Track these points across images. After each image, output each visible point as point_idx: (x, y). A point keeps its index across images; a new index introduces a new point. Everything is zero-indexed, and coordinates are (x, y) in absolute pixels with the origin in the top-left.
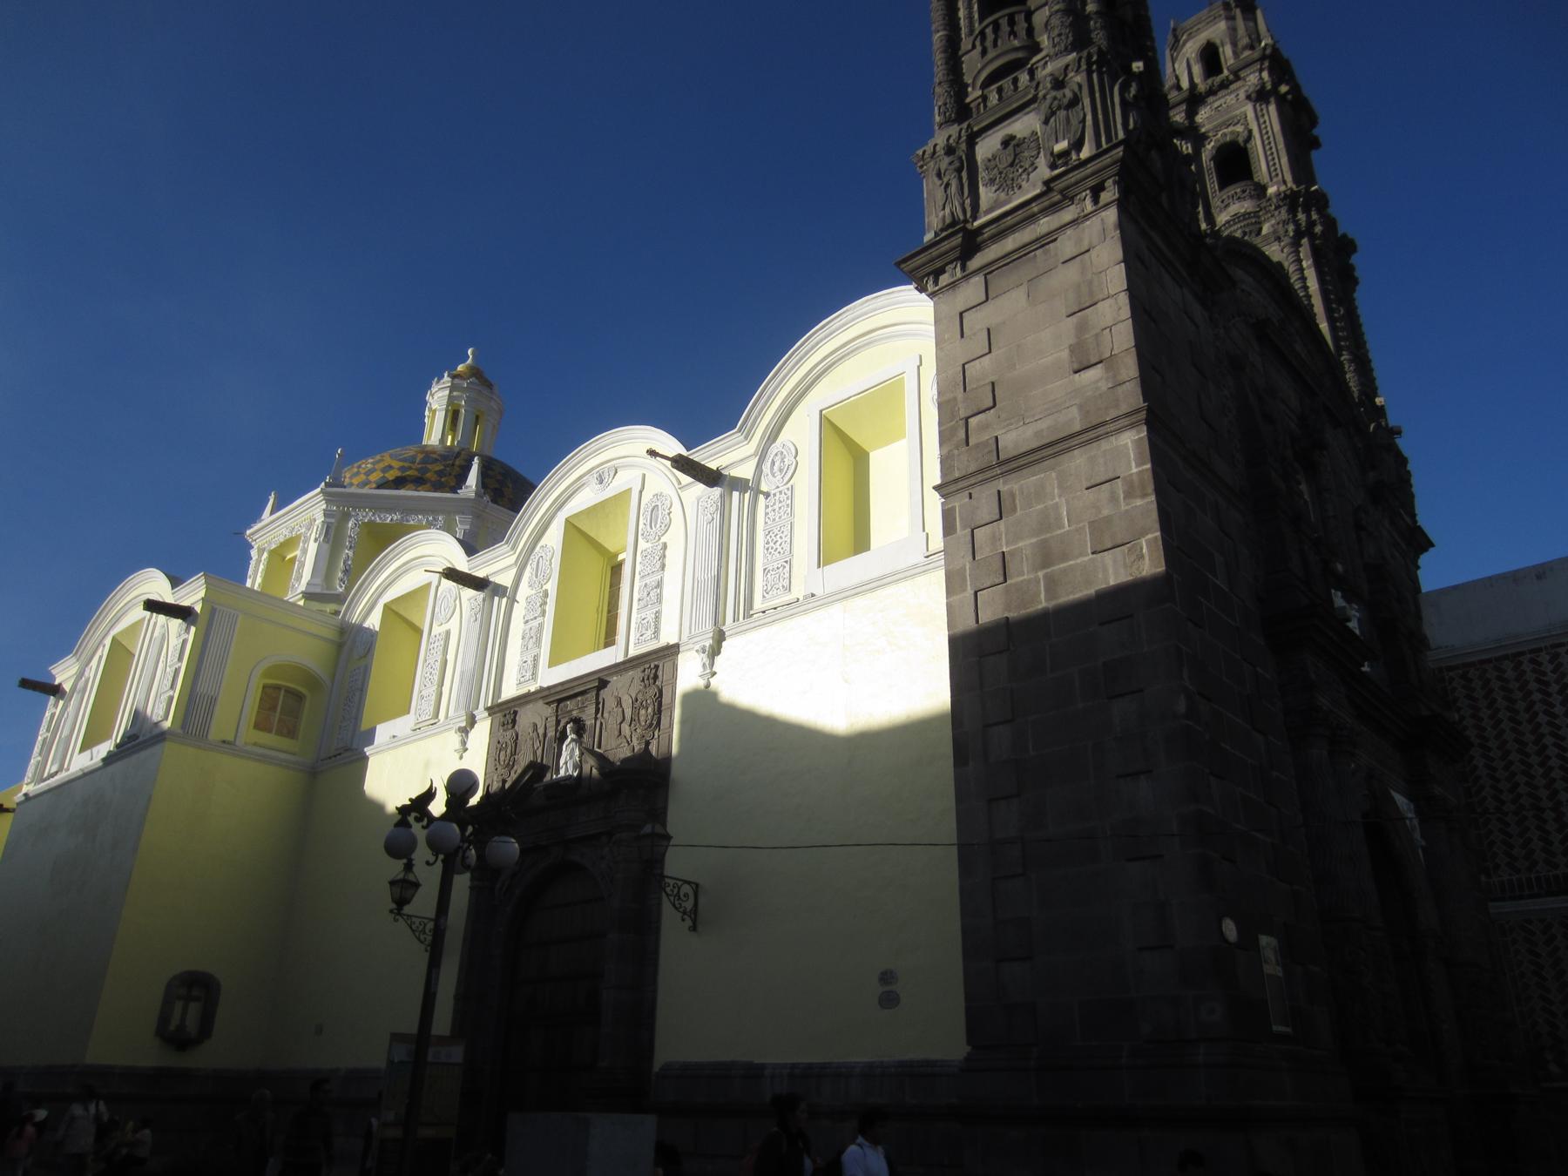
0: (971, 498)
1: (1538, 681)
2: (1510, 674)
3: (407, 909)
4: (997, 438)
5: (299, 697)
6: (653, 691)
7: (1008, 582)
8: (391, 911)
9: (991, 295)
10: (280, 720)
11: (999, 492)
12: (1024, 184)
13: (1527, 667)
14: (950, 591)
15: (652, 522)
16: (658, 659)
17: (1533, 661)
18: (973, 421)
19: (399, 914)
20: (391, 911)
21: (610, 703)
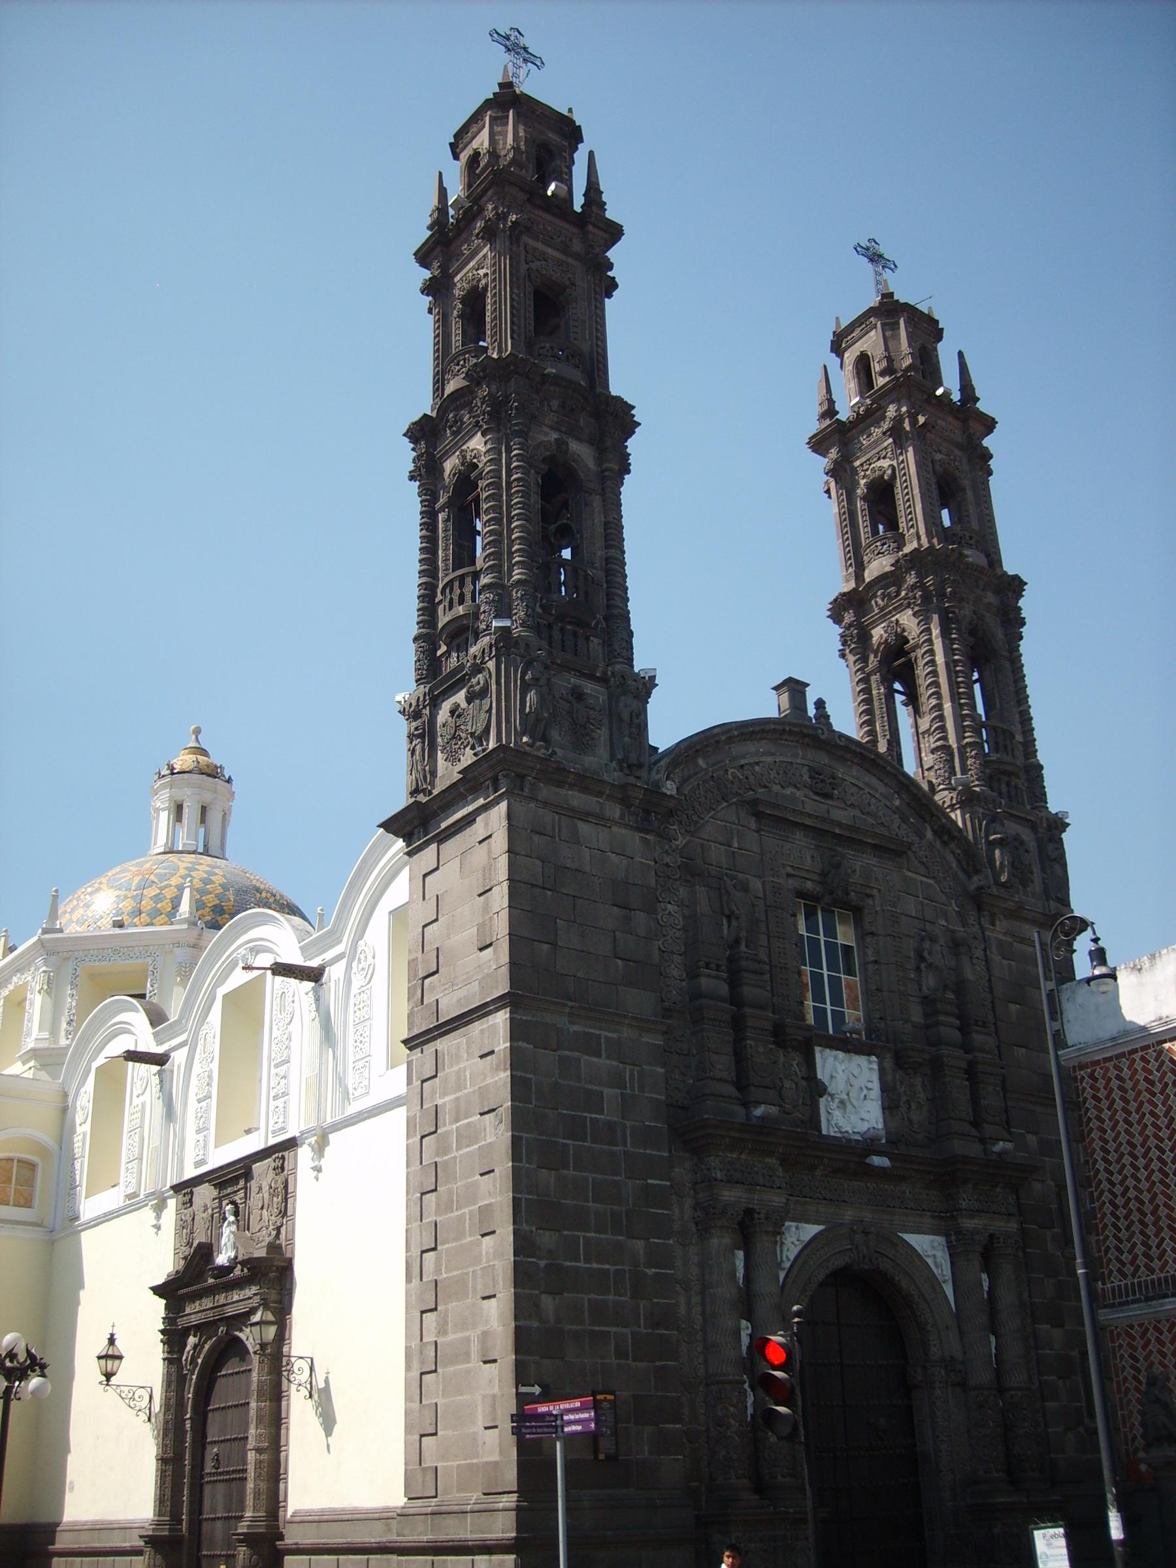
0: (422, 1052)
1: (1146, 1080)
2: (1126, 1073)
3: (114, 1380)
4: (437, 1000)
5: (32, 1166)
6: (280, 1179)
7: (439, 1131)
8: (101, 1383)
9: (441, 864)
10: (15, 1189)
11: (436, 1050)
12: (462, 758)
13: (1139, 1065)
14: (408, 1137)
15: (282, 1008)
16: (285, 1150)
17: (1143, 1059)
18: (427, 981)
19: (107, 1385)
20: (101, 1383)
21: (254, 1189)
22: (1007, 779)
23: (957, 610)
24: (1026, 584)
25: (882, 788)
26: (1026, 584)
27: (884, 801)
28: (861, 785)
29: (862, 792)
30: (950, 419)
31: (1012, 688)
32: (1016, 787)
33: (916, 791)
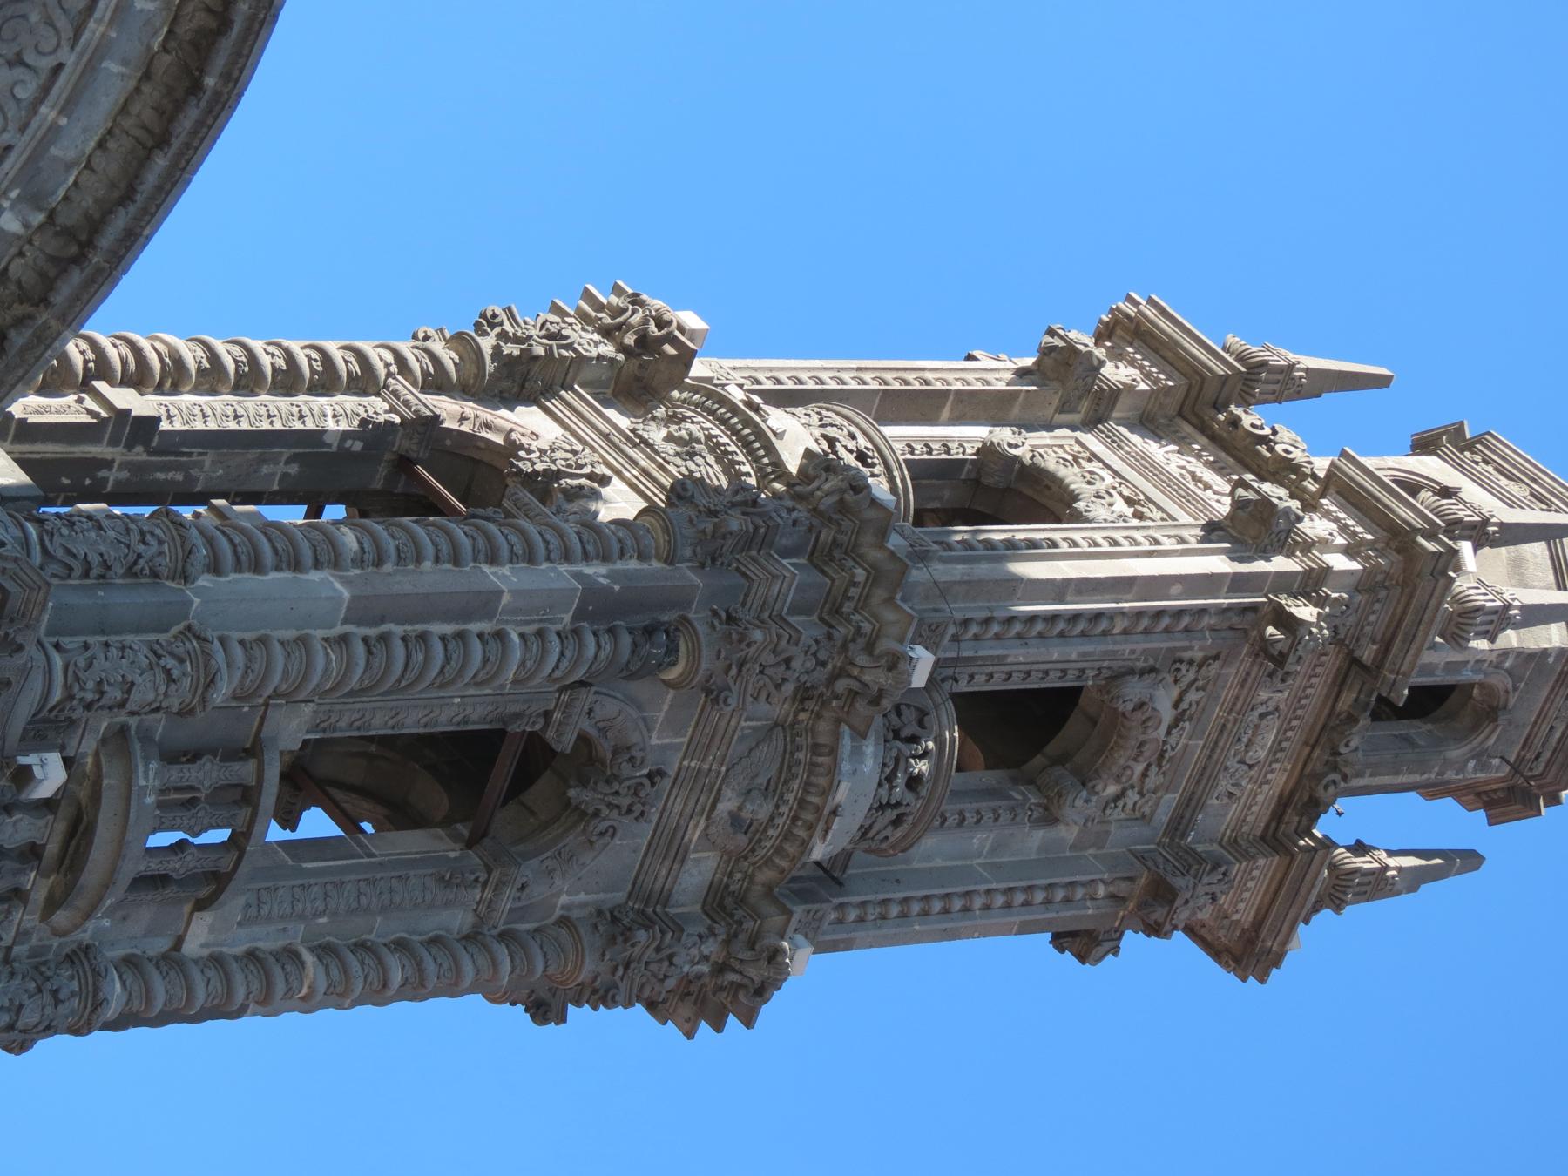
22: (53, 848)
23: (673, 674)
24: (749, 1021)
25: (76, 141)
26: (749, 1021)
27: (23, 145)
28: (94, 30)
29: (67, 31)
30: (1279, 780)
31: (381, 929)
32: (18, 895)
33: (60, 297)
